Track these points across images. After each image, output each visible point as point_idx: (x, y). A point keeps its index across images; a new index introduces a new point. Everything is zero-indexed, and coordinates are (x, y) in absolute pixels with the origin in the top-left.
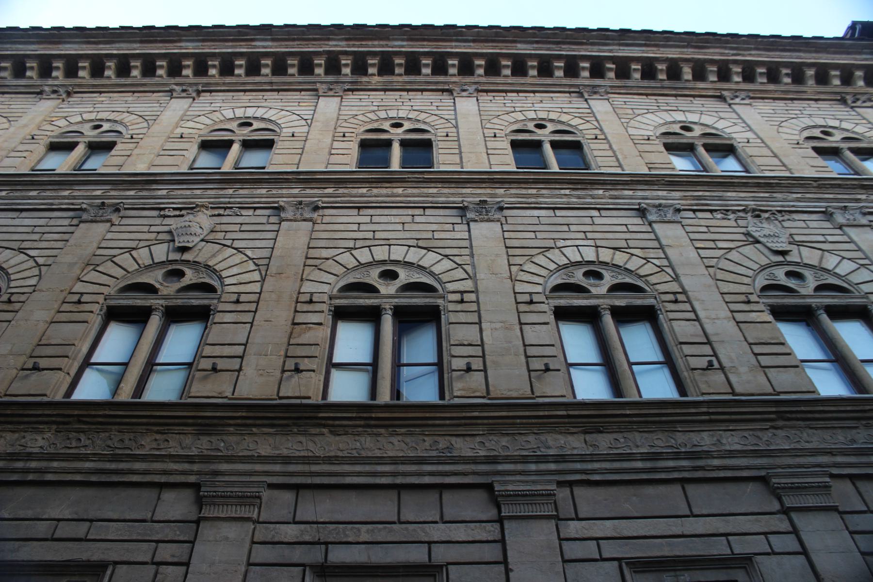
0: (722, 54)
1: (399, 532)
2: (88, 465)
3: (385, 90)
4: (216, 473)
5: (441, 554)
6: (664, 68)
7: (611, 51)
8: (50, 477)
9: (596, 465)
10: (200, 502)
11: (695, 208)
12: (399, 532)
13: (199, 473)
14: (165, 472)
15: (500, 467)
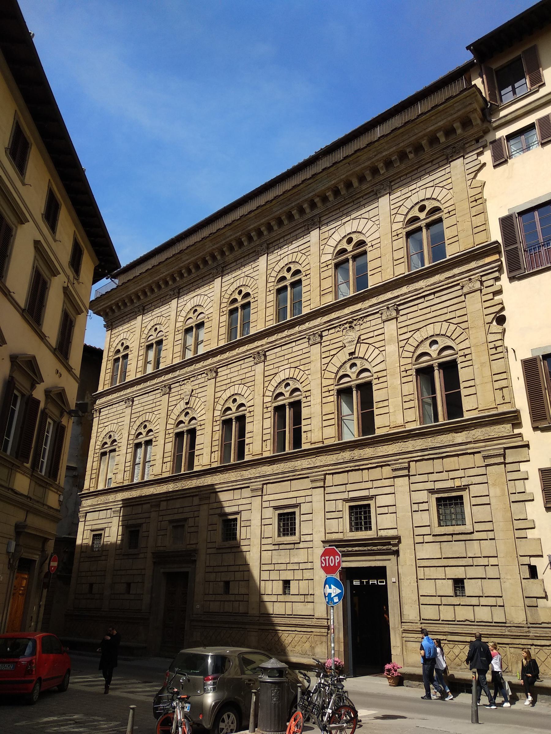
0: (369, 159)
1: (234, 503)
2: (179, 493)
3: (236, 261)
4: (201, 491)
5: (241, 508)
6: (342, 186)
7: (314, 190)
8: (174, 497)
9: (271, 477)
10: (201, 499)
11: (328, 328)
12: (234, 503)
13: (198, 492)
14: (192, 493)
15: (252, 481)
